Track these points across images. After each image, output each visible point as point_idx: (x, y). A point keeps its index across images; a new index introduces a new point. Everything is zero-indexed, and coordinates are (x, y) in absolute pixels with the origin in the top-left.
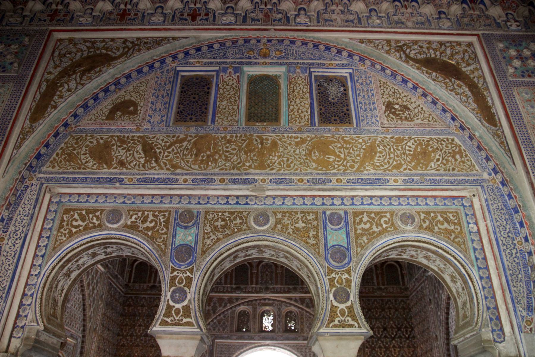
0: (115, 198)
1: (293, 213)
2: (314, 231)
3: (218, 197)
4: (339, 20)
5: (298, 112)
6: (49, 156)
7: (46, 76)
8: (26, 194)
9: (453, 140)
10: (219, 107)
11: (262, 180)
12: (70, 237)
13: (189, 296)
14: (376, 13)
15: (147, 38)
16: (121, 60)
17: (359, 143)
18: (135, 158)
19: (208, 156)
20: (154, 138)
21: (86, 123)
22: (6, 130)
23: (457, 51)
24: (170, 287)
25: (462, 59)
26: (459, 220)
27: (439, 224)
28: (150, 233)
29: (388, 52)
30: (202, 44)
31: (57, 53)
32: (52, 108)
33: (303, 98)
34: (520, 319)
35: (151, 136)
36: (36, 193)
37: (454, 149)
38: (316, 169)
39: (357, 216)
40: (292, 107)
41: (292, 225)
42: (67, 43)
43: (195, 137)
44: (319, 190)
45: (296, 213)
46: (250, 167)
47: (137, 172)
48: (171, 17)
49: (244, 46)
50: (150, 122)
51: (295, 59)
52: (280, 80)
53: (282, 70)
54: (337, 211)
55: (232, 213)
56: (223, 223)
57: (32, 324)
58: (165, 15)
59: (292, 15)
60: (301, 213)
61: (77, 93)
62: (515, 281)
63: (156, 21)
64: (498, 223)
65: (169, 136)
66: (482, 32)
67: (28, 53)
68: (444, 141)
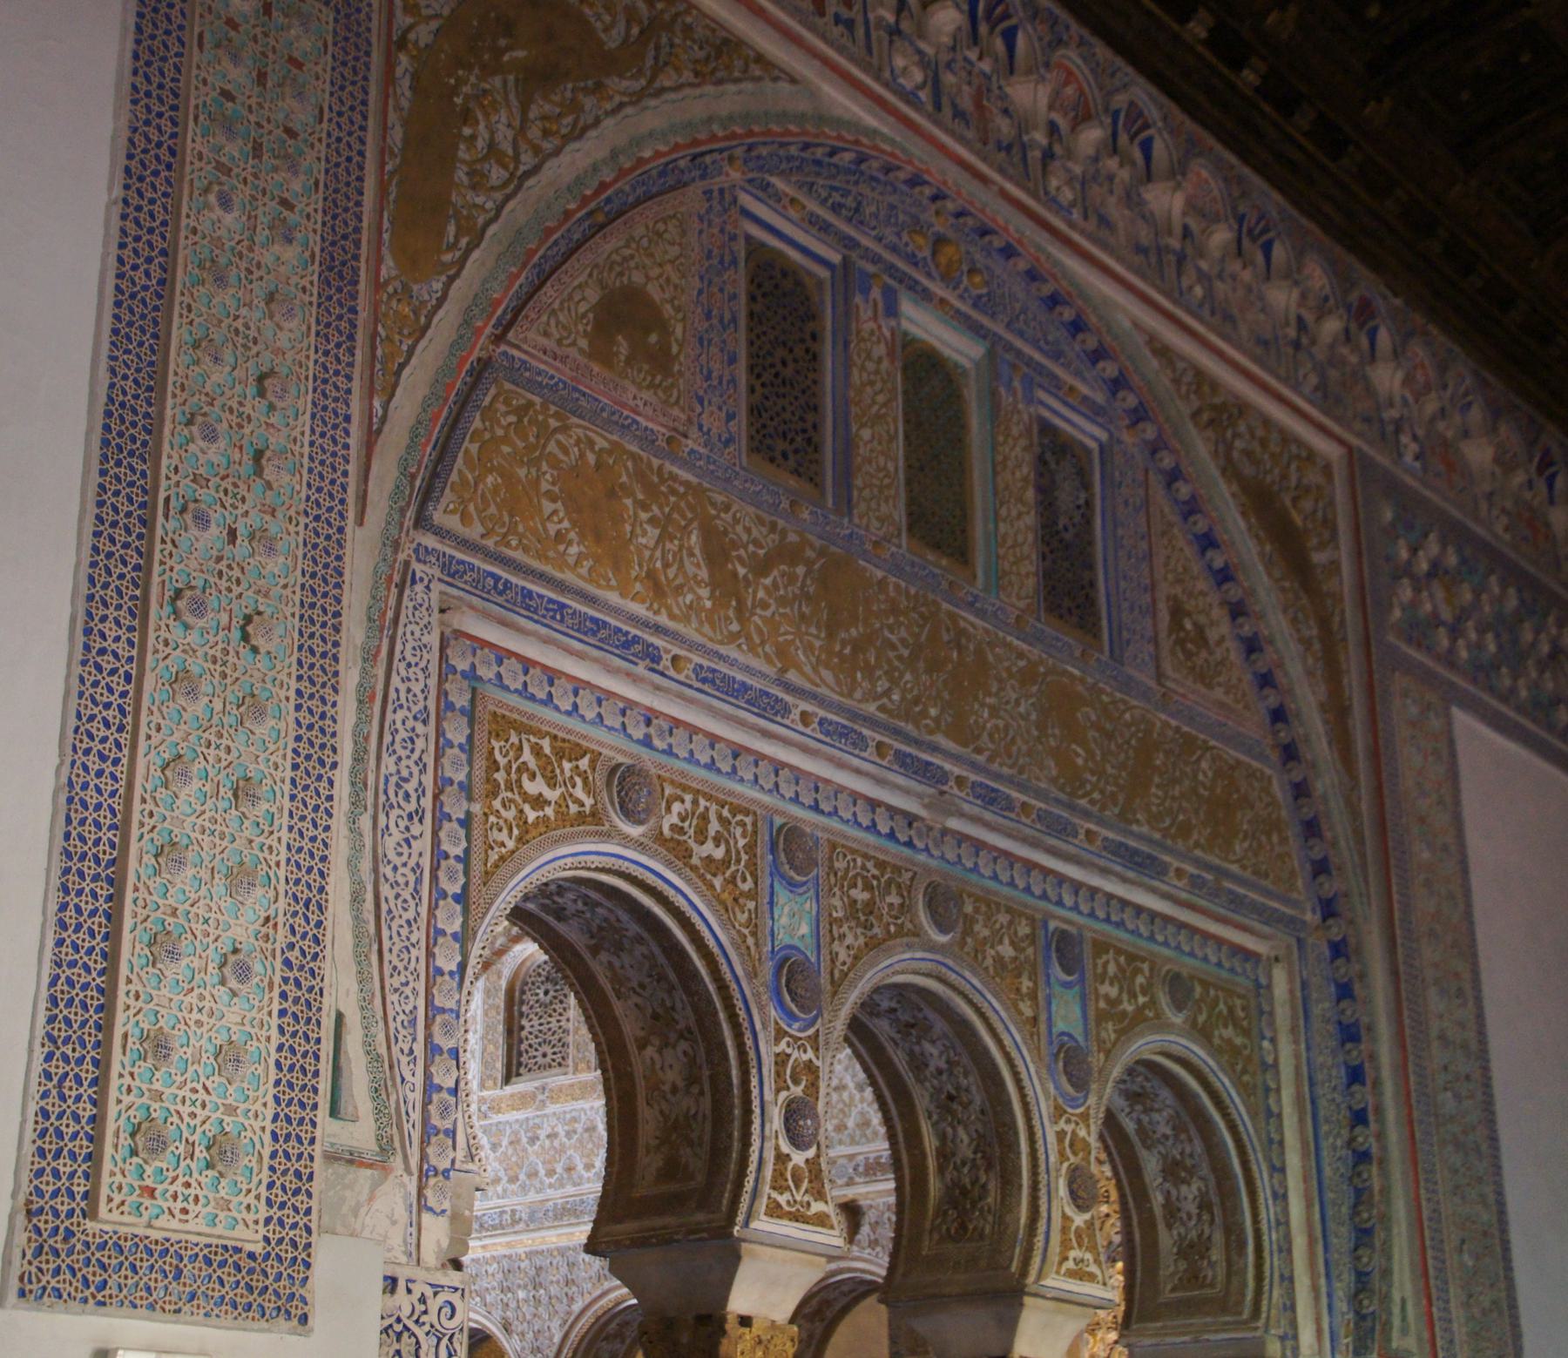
20: (727, 508)
28: (718, 883)
35: (720, 498)
38: (1053, 781)
56: (866, 896)
60: (1009, 910)
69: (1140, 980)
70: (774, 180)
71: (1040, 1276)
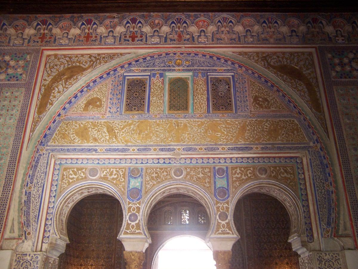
0: (93, 160)
1: (197, 168)
2: (209, 179)
3: (153, 159)
4: (226, 38)
5: (199, 104)
6: (52, 135)
7: (43, 82)
8: (41, 160)
9: (293, 121)
10: (151, 101)
11: (178, 149)
12: (69, 185)
13: (139, 218)
14: (250, 33)
15: (104, 54)
16: (89, 70)
17: (237, 124)
18: (103, 136)
19: (146, 135)
20: (113, 123)
21: (71, 113)
22: (24, 120)
23: (301, 59)
24: (129, 213)
25: (304, 65)
26: (294, 171)
27: (281, 175)
28: (115, 182)
29: (256, 61)
30: (139, 58)
31: (48, 66)
32: (50, 105)
33: (202, 94)
34: (322, 229)
35: (111, 122)
36: (47, 159)
37: (293, 127)
38: (210, 141)
39: (234, 170)
40: (196, 101)
41: (196, 176)
42: (54, 58)
43: (138, 122)
44: (212, 154)
45: (198, 168)
46: (171, 141)
47: (105, 145)
48: (119, 38)
49: (166, 57)
50: (110, 112)
51: (198, 67)
52: (188, 81)
53: (190, 74)
54: (222, 167)
55: (161, 169)
56: (156, 175)
57: (53, 235)
58: (114, 37)
59: (196, 36)
61: (64, 94)
62: (322, 208)
63: (109, 42)
64: (316, 174)
65: (122, 122)
66: (318, 45)
67: (30, 66)
68: (288, 122)
69: (248, 172)
70: (132, 69)
71: (211, 235)
